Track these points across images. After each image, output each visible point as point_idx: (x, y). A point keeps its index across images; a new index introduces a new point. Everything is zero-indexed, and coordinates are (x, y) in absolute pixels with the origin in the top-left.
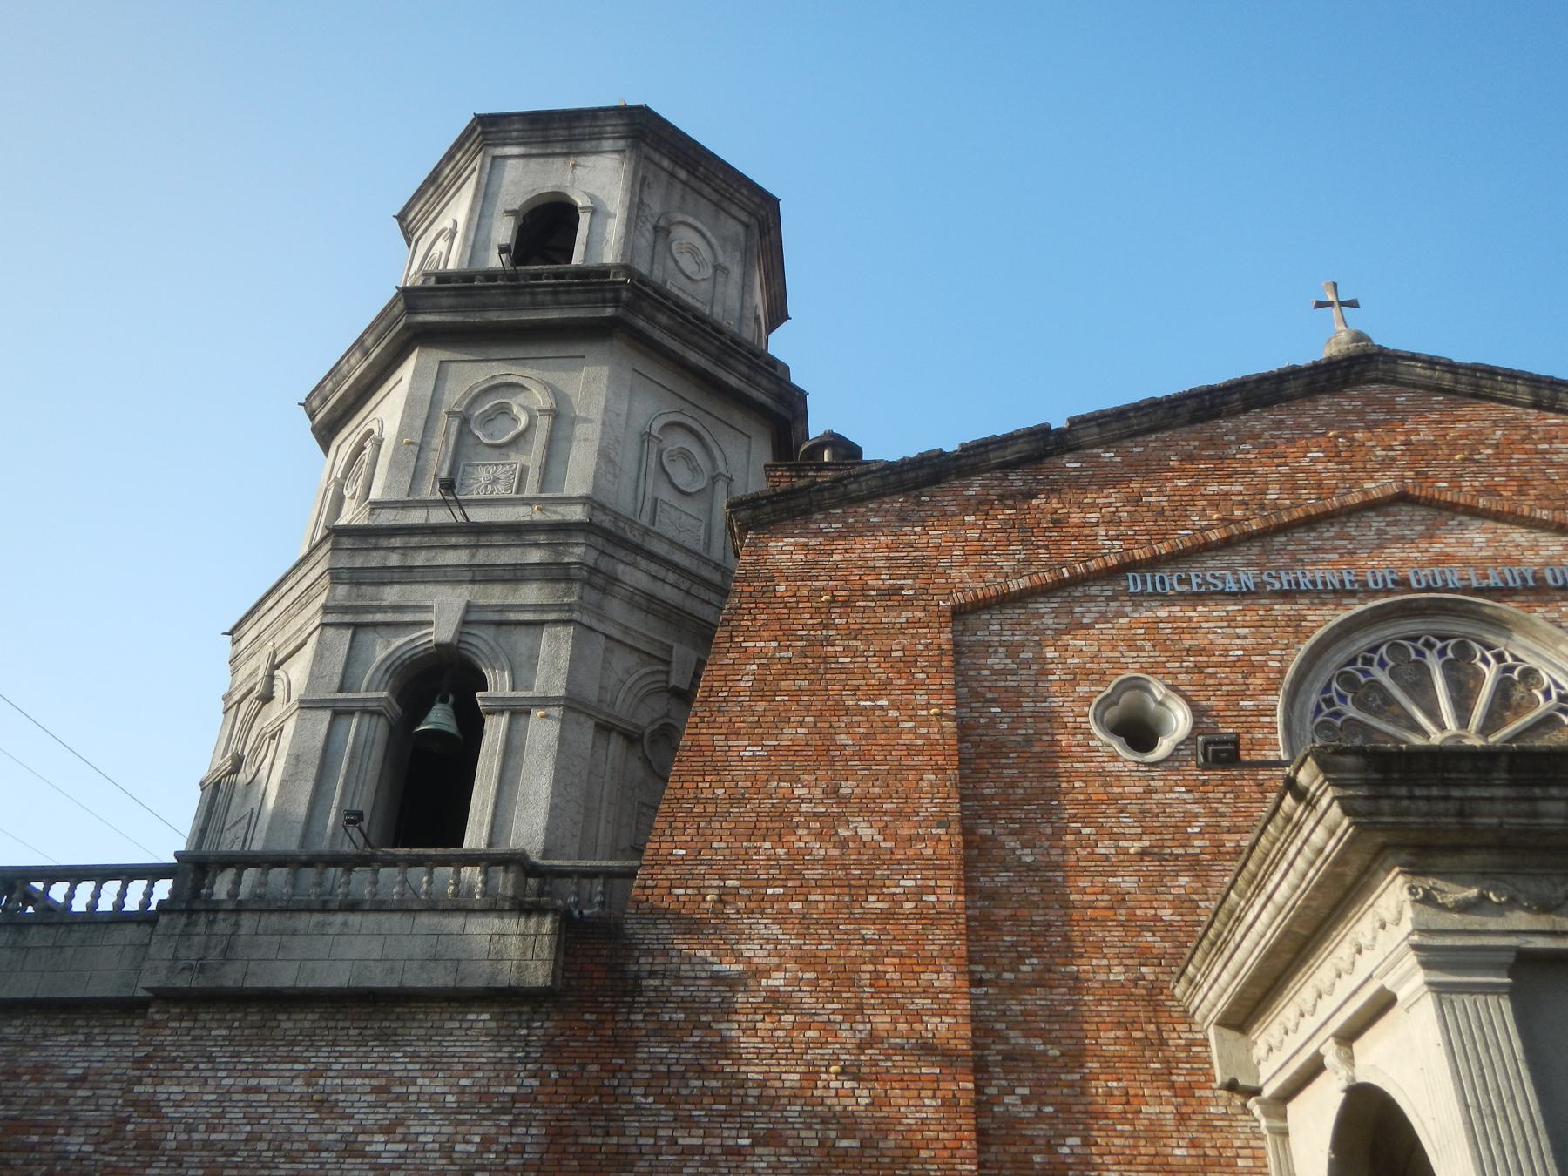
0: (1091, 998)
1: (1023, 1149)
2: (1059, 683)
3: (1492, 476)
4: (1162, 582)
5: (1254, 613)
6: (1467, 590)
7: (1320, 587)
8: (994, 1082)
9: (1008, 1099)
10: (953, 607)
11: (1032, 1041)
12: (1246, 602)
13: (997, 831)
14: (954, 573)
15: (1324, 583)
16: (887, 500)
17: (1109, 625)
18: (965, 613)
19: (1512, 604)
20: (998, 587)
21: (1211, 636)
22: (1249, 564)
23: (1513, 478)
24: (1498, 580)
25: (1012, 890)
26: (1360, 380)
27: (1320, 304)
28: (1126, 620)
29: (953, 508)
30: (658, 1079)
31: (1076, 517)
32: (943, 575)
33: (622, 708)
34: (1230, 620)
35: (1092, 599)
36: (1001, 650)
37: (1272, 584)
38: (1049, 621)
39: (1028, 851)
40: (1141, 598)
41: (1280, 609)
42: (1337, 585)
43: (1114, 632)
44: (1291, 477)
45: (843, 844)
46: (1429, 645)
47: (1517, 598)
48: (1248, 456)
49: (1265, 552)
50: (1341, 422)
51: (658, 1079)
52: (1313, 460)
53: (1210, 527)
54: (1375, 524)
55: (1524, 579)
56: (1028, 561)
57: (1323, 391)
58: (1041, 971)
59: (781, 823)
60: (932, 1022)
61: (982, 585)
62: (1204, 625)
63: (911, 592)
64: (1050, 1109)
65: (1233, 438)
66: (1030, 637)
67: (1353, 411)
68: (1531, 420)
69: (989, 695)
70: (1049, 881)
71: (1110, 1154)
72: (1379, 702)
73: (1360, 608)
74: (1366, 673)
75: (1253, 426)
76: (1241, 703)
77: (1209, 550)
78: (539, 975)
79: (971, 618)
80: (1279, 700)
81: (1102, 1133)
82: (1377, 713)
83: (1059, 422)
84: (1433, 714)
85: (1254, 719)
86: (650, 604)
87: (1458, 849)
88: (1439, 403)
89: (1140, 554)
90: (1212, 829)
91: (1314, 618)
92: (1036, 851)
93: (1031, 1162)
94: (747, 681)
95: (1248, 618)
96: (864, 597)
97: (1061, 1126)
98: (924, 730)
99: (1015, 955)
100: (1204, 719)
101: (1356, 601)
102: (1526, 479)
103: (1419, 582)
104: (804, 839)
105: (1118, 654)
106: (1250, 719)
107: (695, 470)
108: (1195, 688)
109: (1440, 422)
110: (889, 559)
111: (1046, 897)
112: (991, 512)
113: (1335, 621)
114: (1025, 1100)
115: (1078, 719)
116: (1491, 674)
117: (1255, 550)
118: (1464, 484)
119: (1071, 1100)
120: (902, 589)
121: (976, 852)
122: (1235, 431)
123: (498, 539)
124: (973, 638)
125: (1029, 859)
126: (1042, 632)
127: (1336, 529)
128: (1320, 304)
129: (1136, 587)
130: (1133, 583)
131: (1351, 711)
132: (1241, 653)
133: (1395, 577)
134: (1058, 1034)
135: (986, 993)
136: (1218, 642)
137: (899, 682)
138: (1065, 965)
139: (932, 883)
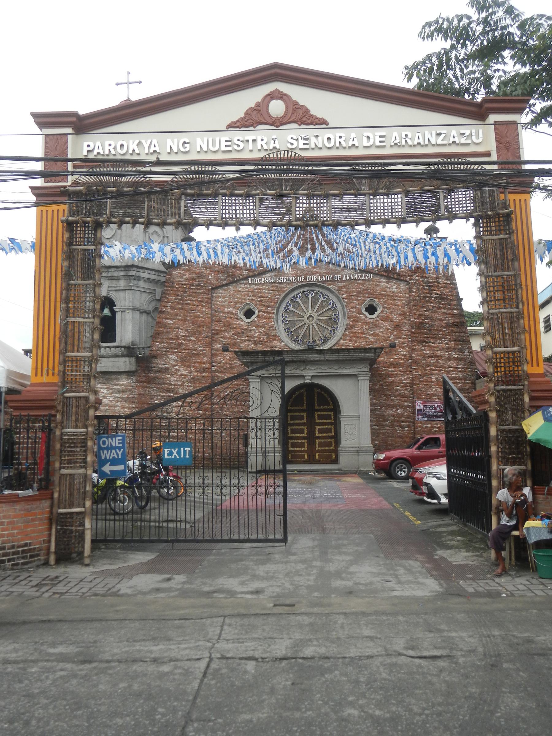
30: (157, 385)
32: (210, 280)
33: (145, 307)
34: (269, 289)
35: (241, 284)
41: (281, 286)
45: (189, 341)
51: (157, 385)
56: (229, 276)
59: (177, 338)
60: (204, 374)
78: (134, 369)
79: (216, 291)
80: (275, 308)
84: (307, 308)
86: (149, 280)
89: (251, 274)
90: (259, 336)
94: (169, 306)
96: (193, 286)
104: (181, 340)
107: (159, 235)
116: (321, 299)
123: (113, 269)
126: (230, 293)
131: (291, 308)
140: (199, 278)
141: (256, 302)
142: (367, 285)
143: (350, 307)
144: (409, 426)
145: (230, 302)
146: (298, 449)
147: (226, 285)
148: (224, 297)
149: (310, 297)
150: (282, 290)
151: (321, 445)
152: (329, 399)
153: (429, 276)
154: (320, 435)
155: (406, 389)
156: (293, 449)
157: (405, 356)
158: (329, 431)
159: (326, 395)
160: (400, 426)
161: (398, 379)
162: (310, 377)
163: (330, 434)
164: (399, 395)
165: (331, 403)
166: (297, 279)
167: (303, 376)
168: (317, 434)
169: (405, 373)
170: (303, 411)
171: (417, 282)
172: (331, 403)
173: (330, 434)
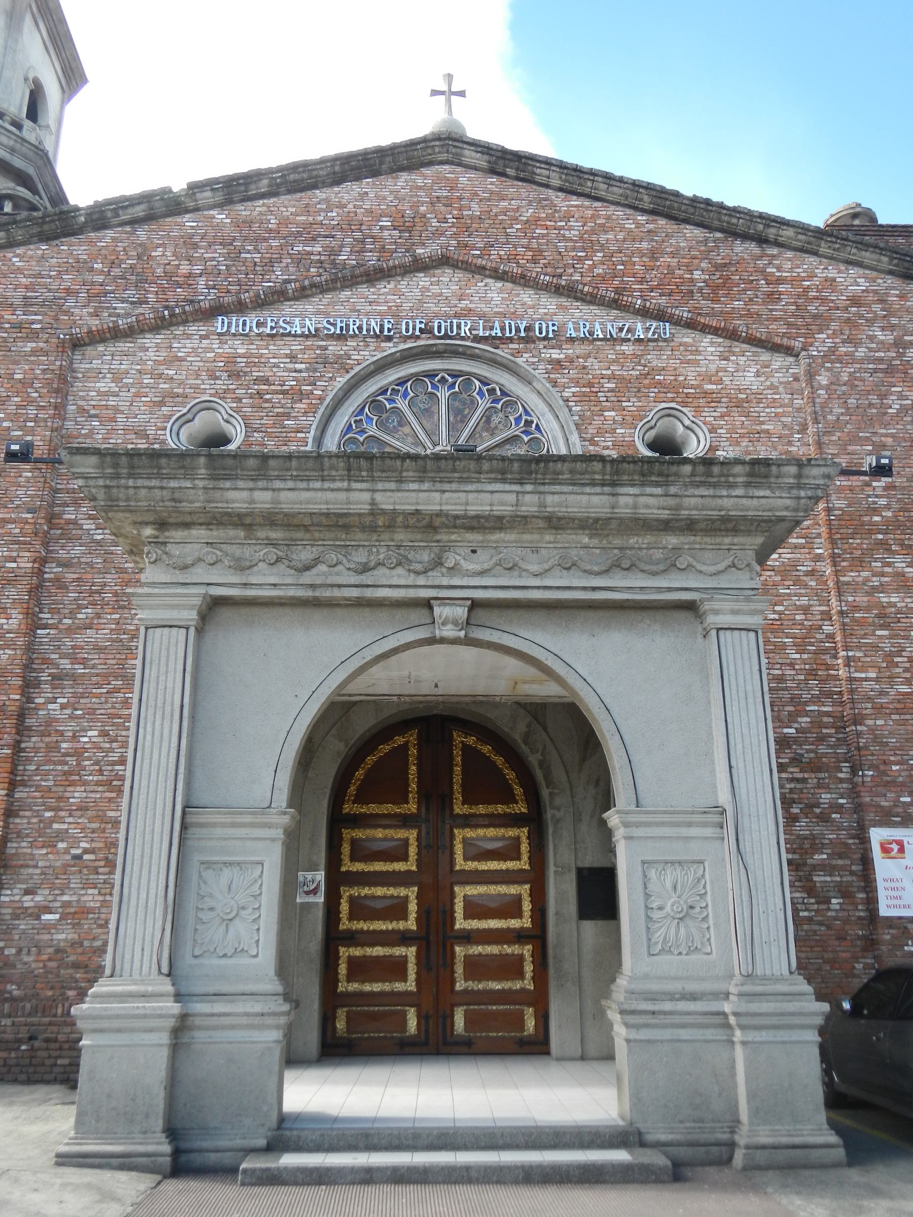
0: (126, 636)
1: (55, 739)
2: (148, 404)
3: (515, 247)
4: (244, 324)
5: (312, 352)
6: (477, 339)
7: (365, 332)
8: (42, 695)
9: (51, 706)
10: (71, 340)
11: (76, 666)
12: (308, 343)
13: (79, 516)
14: (76, 311)
15: (368, 330)
16: (32, 247)
17: (199, 359)
18: (85, 345)
19: (506, 351)
20: (111, 325)
21: (274, 370)
22: (318, 313)
23: (531, 249)
24: (498, 331)
25: (82, 560)
26: (430, 163)
27: (435, 93)
28: (212, 355)
29: (85, 257)
31: (185, 268)
32: (66, 313)
34: (292, 357)
35: (189, 337)
36: (108, 376)
37: (329, 330)
38: (151, 354)
39: (100, 531)
40: (228, 338)
41: (334, 348)
42: (378, 333)
43: (201, 364)
44: (363, 242)
46: (443, 380)
47: (511, 346)
48: (332, 222)
49: (332, 304)
50: (412, 196)
52: (382, 228)
53: (288, 281)
54: (421, 283)
55: (518, 330)
57: (402, 169)
58: (92, 618)
61: (98, 322)
62: (272, 360)
63: (39, 326)
64: (80, 712)
65: (324, 206)
66: (133, 367)
67: (420, 188)
68: (557, 201)
69: (92, 412)
70: (112, 554)
71: (117, 742)
72: (395, 424)
73: (393, 350)
74: (391, 401)
75: (342, 197)
76: (286, 422)
77: (289, 300)
79: (89, 351)
80: (314, 421)
81: (114, 728)
82: (391, 432)
83: (178, 185)
85: (293, 435)
87: (187, 525)
88: (492, 184)
89: (228, 299)
91: (357, 357)
92: (106, 531)
93: (59, 748)
95: (306, 356)
97: (86, 724)
98: (29, 438)
99: (75, 606)
100: (255, 434)
101: (391, 344)
102: (541, 251)
103: (439, 331)
105: (199, 382)
106: (289, 435)
108: (254, 410)
109: (489, 200)
110: (25, 297)
111: (107, 565)
112: (116, 261)
113: (375, 358)
114: (63, 707)
115: (159, 432)
116: (483, 404)
117: (325, 301)
118: (492, 252)
119: (96, 706)
120: (32, 323)
121: (59, 532)
122: (327, 201)
124: (88, 366)
125: (99, 537)
126: (142, 362)
127: (392, 285)
128: (435, 93)
129: (223, 326)
130: (220, 323)
132: (295, 383)
133: (423, 326)
134: (96, 661)
135: (48, 634)
136: (279, 374)
137: (16, 399)
138: (110, 614)
139: (15, 554)
140: (27, 302)
141: (240, 400)
142: (654, 360)
143: (592, 430)
144: (845, 893)
145: (137, 395)
146: (377, 987)
147: (130, 333)
148: (117, 378)
149: (443, 394)
150: (342, 364)
151: (475, 968)
152: (510, 775)
153: (871, 338)
154: (475, 924)
155: (822, 739)
156: (354, 987)
157: (806, 610)
158: (512, 908)
159: (499, 761)
160: (810, 890)
161: (786, 695)
162: (461, 612)
163: (514, 923)
164: (796, 760)
165: (518, 790)
166: (396, 326)
167: (427, 604)
168: (461, 923)
169: (812, 674)
170: (405, 821)
171: (830, 355)
172: (518, 790)
173: (514, 923)
